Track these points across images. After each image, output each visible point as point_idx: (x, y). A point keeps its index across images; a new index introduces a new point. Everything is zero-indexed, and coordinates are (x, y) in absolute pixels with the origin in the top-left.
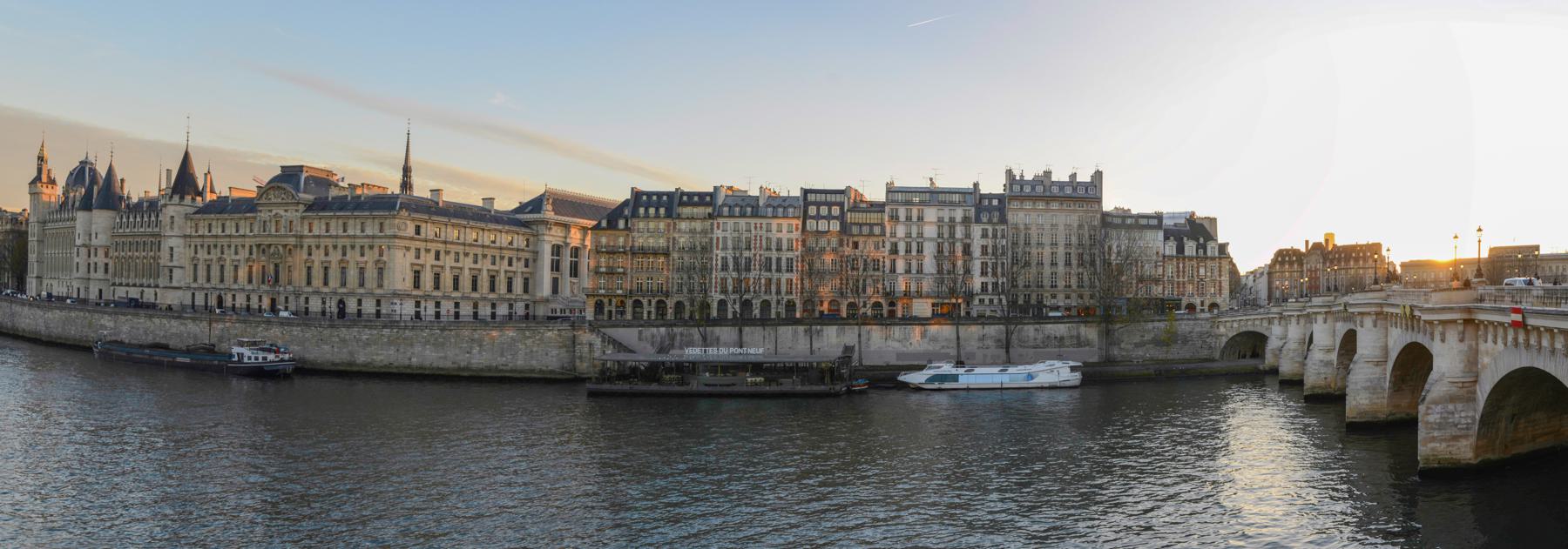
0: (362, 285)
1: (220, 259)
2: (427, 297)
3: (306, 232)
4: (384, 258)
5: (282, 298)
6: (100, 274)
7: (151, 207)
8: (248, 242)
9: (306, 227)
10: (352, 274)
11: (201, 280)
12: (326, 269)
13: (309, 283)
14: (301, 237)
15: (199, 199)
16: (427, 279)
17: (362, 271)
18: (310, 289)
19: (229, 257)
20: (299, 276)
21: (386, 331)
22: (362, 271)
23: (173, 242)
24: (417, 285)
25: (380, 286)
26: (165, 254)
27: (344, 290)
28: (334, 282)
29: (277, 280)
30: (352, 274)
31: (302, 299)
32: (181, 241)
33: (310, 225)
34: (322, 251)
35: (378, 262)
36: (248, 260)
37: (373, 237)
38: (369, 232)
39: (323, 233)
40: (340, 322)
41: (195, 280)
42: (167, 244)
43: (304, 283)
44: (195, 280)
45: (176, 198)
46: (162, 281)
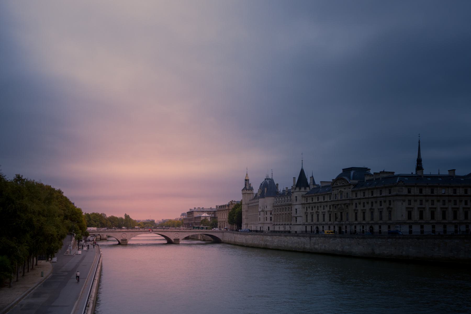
0: (381, 219)
1: (317, 212)
2: (416, 223)
3: (354, 197)
4: (391, 206)
5: (344, 227)
6: (269, 221)
7: (288, 193)
8: (329, 204)
9: (354, 195)
10: (376, 214)
11: (309, 221)
12: (364, 213)
13: (356, 219)
14: (352, 200)
15: (308, 188)
16: (416, 215)
17: (381, 212)
18: (356, 222)
19: (321, 210)
20: (352, 218)
21: (389, 240)
22: (381, 212)
23: (297, 207)
24: (410, 217)
25: (390, 219)
26: (294, 212)
27: (373, 222)
28: (368, 218)
29: (342, 219)
30: (376, 214)
31: (353, 227)
32: (300, 206)
33: (356, 194)
34: (362, 205)
35: (388, 208)
36: (329, 211)
37: (386, 197)
38: (383, 194)
39: (362, 197)
40: (236, 232)
41: (307, 221)
42: (294, 208)
43: (354, 219)
44: (307, 221)
45: (298, 189)
46: (293, 222)
